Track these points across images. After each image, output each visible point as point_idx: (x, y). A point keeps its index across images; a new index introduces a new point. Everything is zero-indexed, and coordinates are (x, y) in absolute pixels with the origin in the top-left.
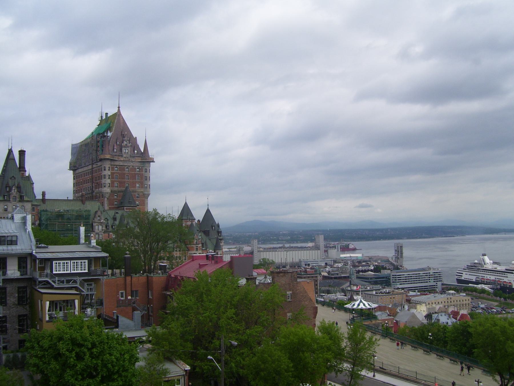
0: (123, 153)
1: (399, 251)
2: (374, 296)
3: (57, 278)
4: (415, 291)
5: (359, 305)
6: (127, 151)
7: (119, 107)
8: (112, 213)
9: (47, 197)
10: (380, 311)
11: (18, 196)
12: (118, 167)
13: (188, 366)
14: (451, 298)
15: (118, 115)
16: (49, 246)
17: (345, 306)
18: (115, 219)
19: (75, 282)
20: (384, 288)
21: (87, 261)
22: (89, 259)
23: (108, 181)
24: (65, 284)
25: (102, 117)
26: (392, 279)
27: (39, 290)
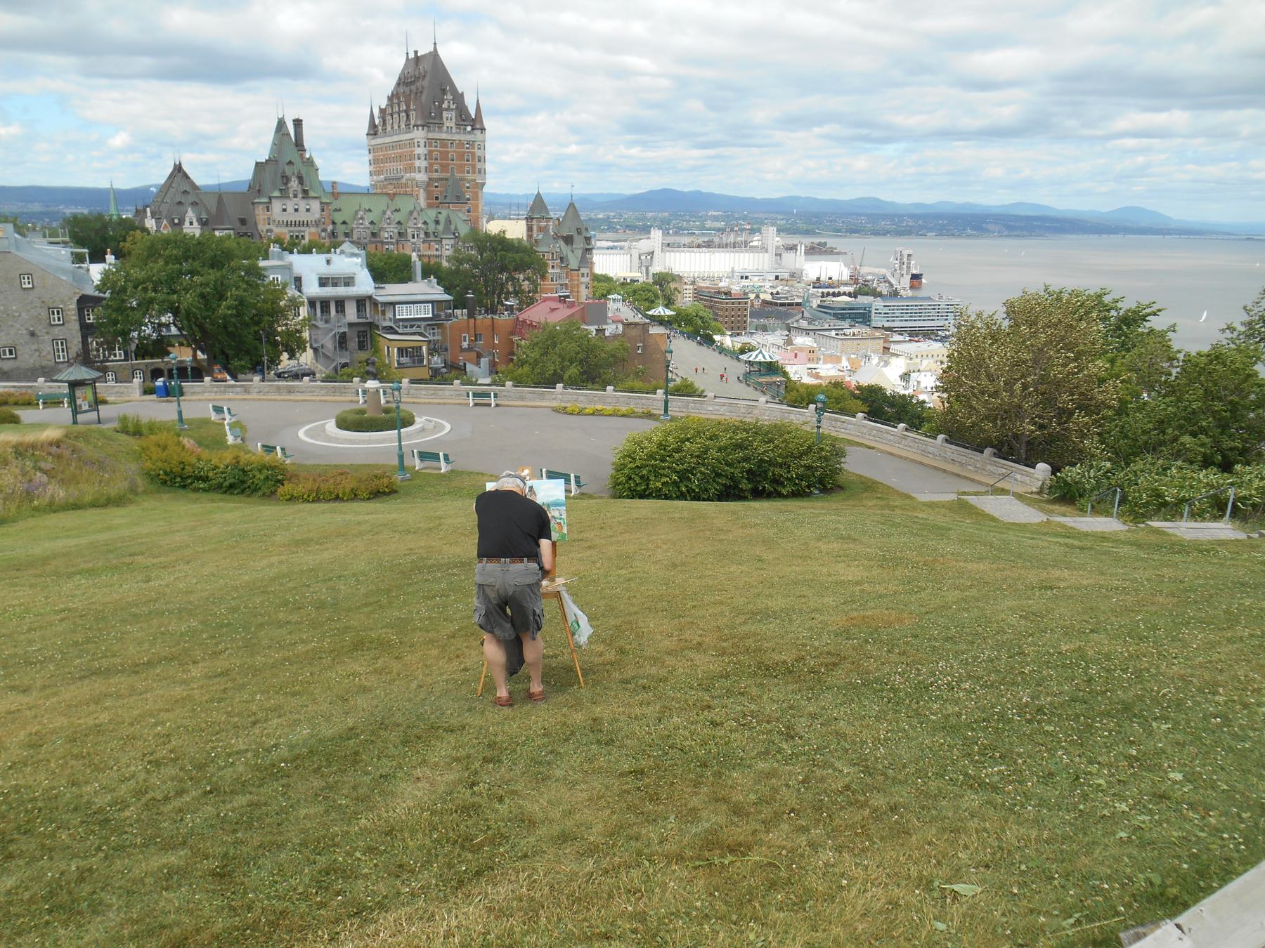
0: (445, 119)
2: (832, 340)
4: (902, 335)
7: (435, 44)
8: (432, 214)
9: (339, 190)
10: (831, 362)
11: (299, 189)
15: (434, 55)
16: (386, 285)
18: (437, 222)
19: (419, 326)
20: (852, 326)
22: (432, 302)
23: (422, 163)
26: (873, 311)
27: (385, 335)
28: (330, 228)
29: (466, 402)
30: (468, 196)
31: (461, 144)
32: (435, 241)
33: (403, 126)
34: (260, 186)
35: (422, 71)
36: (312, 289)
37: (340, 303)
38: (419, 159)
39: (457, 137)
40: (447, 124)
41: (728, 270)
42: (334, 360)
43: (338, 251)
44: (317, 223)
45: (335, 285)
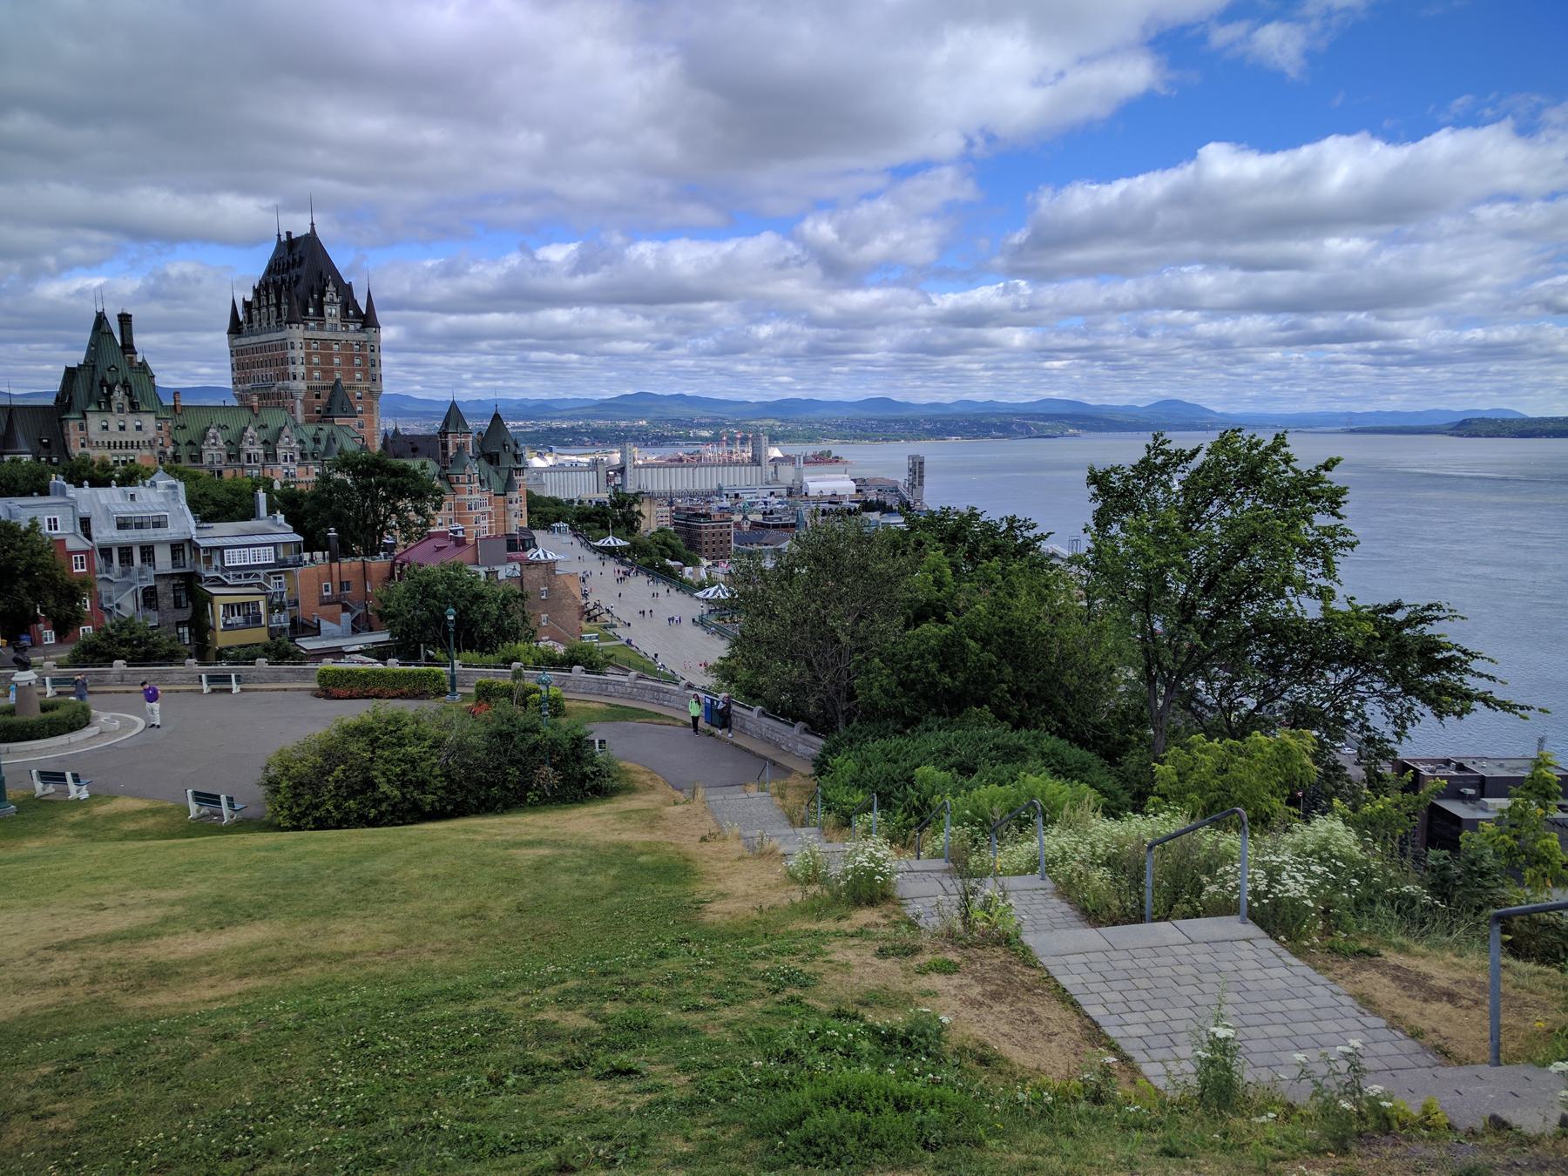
1: (917, 469)
7: (312, 224)
8: (311, 430)
11: (126, 402)
18: (317, 441)
19: (257, 576)
22: (275, 545)
28: (170, 450)
29: (198, 687)
30: (359, 408)
31: (348, 345)
33: (273, 323)
34: (70, 398)
35: (297, 257)
36: (106, 533)
37: (148, 551)
39: (343, 336)
40: (329, 321)
41: (715, 487)
43: (148, 482)
44: (151, 444)
45: (140, 526)
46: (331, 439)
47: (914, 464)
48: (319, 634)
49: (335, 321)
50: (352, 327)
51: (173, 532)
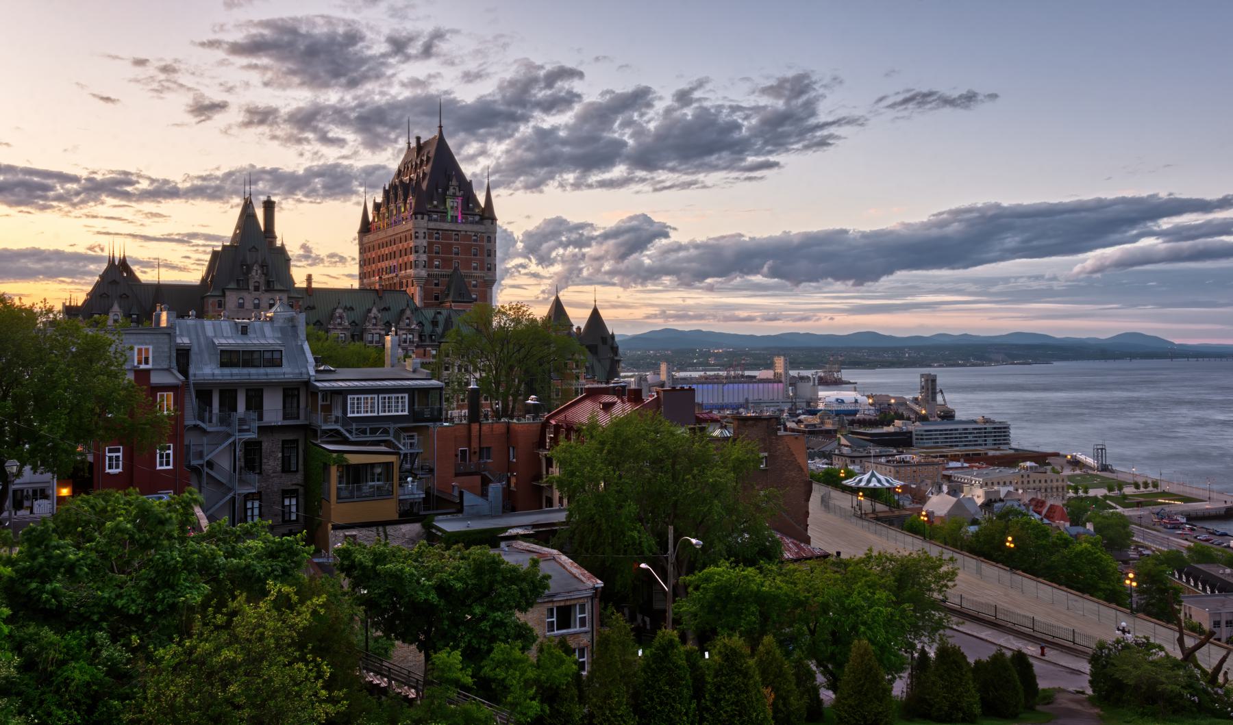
0: (449, 209)
2: (884, 467)
3: (354, 424)
4: (959, 461)
5: (869, 481)
6: (455, 204)
8: (430, 313)
9: (314, 285)
11: (262, 281)
12: (440, 232)
13: (599, 582)
14: (1028, 476)
16: (339, 370)
17: (844, 482)
18: (435, 323)
19: (386, 431)
20: (902, 453)
21: (406, 395)
22: (411, 391)
24: (368, 435)
25: (409, 143)
26: (914, 437)
27: (323, 446)
30: (474, 296)
31: (467, 237)
32: (431, 346)
36: (206, 370)
38: (416, 252)
40: (450, 213)
41: (742, 400)
42: (230, 490)
45: (246, 364)
46: (448, 323)
47: (927, 381)
48: (460, 511)
49: (456, 214)
50: (470, 219)
51: (287, 372)
